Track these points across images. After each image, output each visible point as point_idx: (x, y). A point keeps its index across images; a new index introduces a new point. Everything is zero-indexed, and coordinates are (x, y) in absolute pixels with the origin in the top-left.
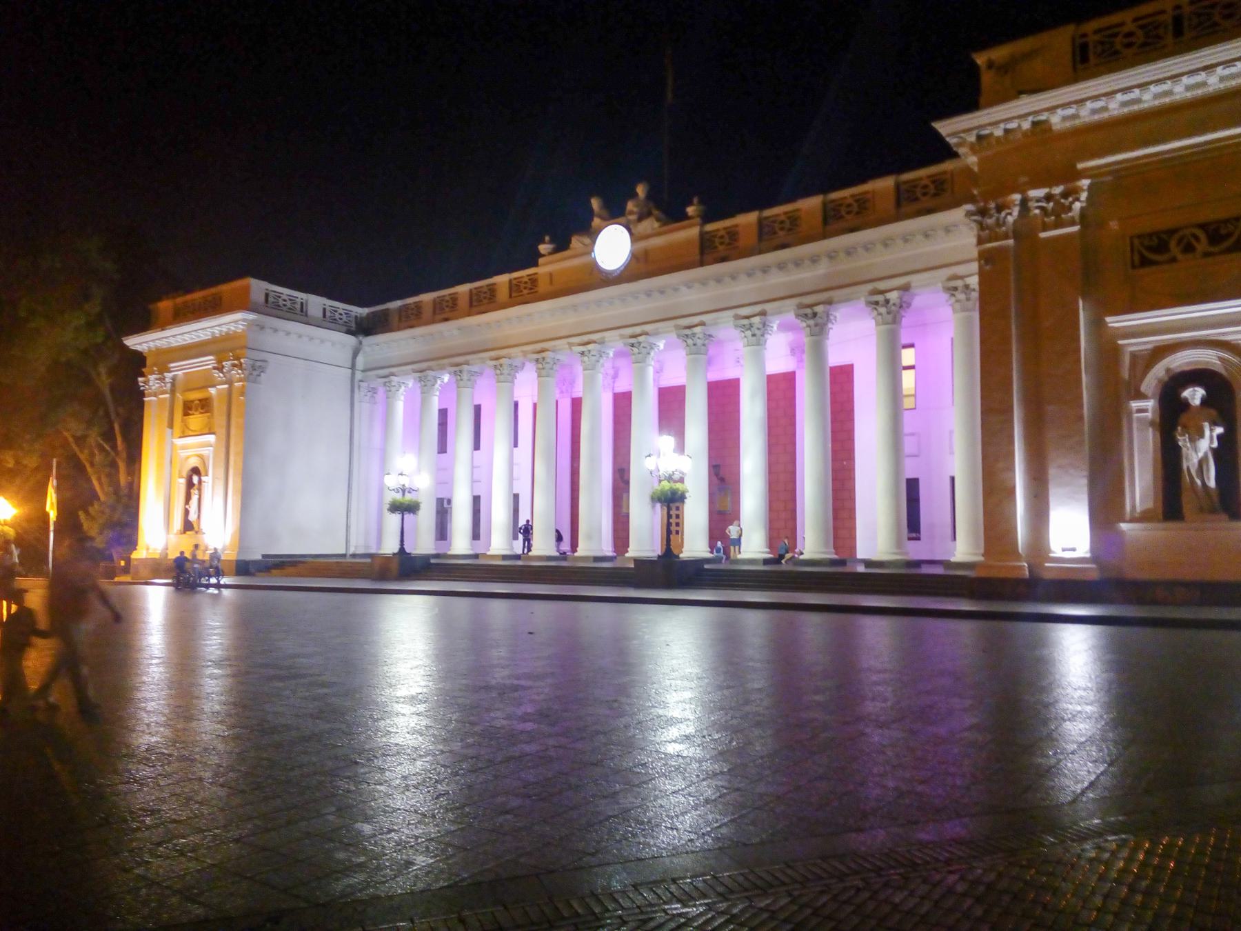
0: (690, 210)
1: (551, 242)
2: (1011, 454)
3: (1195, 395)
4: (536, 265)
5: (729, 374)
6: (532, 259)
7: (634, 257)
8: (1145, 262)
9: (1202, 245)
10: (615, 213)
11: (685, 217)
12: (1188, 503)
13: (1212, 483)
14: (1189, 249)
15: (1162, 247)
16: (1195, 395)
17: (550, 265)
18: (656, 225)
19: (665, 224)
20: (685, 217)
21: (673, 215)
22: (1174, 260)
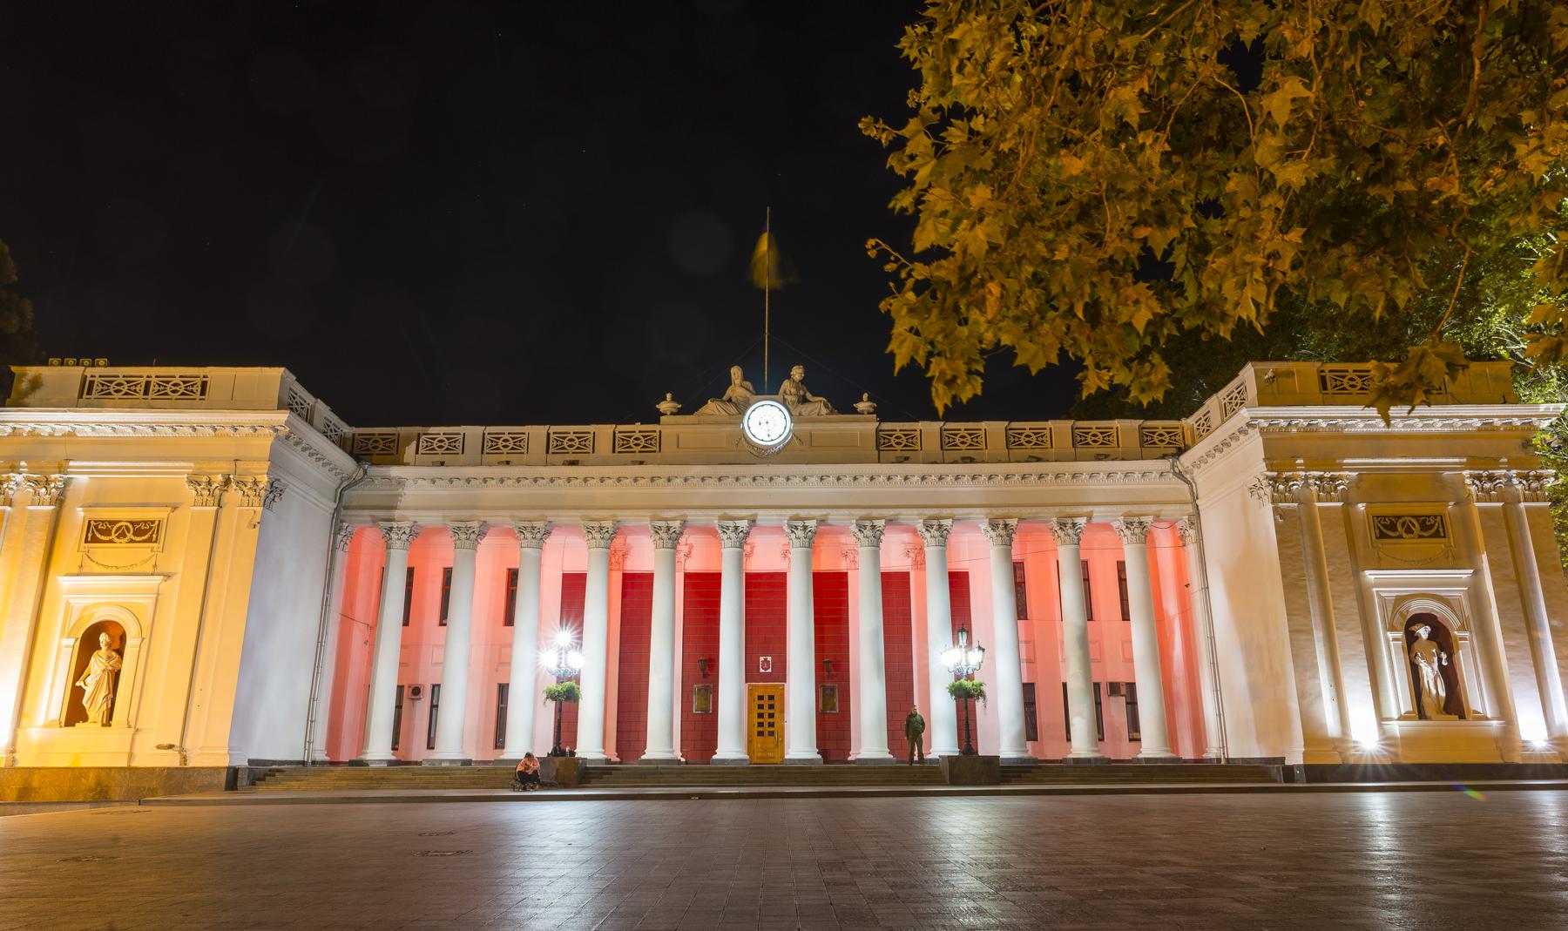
0: (861, 406)
1: (673, 400)
2: (1315, 666)
3: (1423, 632)
4: (658, 422)
5: (843, 566)
6: (654, 417)
7: (795, 435)
8: (1383, 536)
9: (1417, 530)
10: (765, 387)
11: (855, 411)
12: (1429, 711)
13: (1442, 694)
14: (1409, 531)
15: (1393, 527)
16: (1423, 632)
17: (672, 427)
18: (824, 411)
19: (831, 413)
20: (855, 411)
21: (843, 405)
22: (1400, 537)
